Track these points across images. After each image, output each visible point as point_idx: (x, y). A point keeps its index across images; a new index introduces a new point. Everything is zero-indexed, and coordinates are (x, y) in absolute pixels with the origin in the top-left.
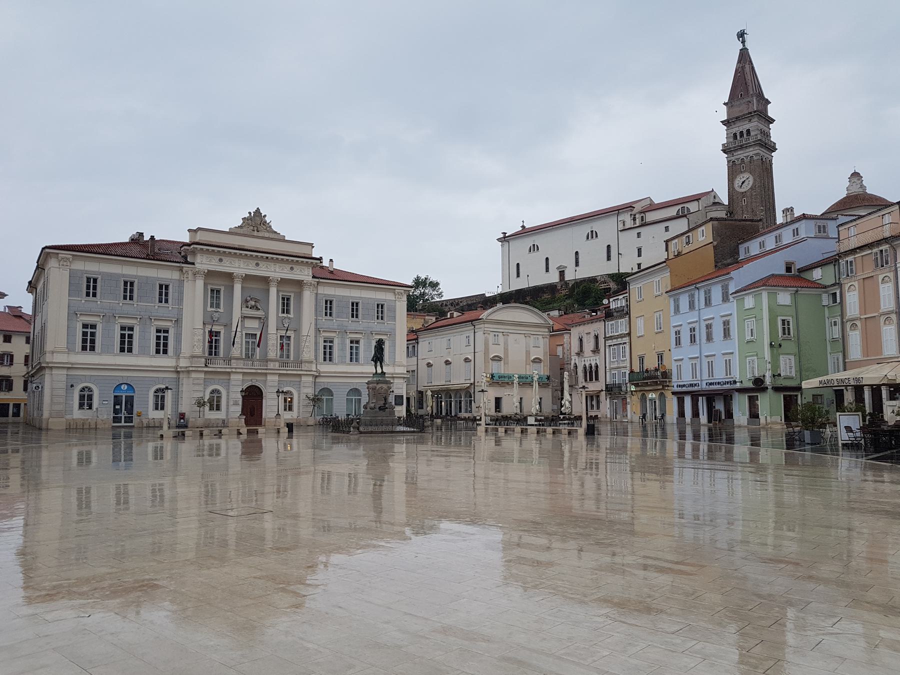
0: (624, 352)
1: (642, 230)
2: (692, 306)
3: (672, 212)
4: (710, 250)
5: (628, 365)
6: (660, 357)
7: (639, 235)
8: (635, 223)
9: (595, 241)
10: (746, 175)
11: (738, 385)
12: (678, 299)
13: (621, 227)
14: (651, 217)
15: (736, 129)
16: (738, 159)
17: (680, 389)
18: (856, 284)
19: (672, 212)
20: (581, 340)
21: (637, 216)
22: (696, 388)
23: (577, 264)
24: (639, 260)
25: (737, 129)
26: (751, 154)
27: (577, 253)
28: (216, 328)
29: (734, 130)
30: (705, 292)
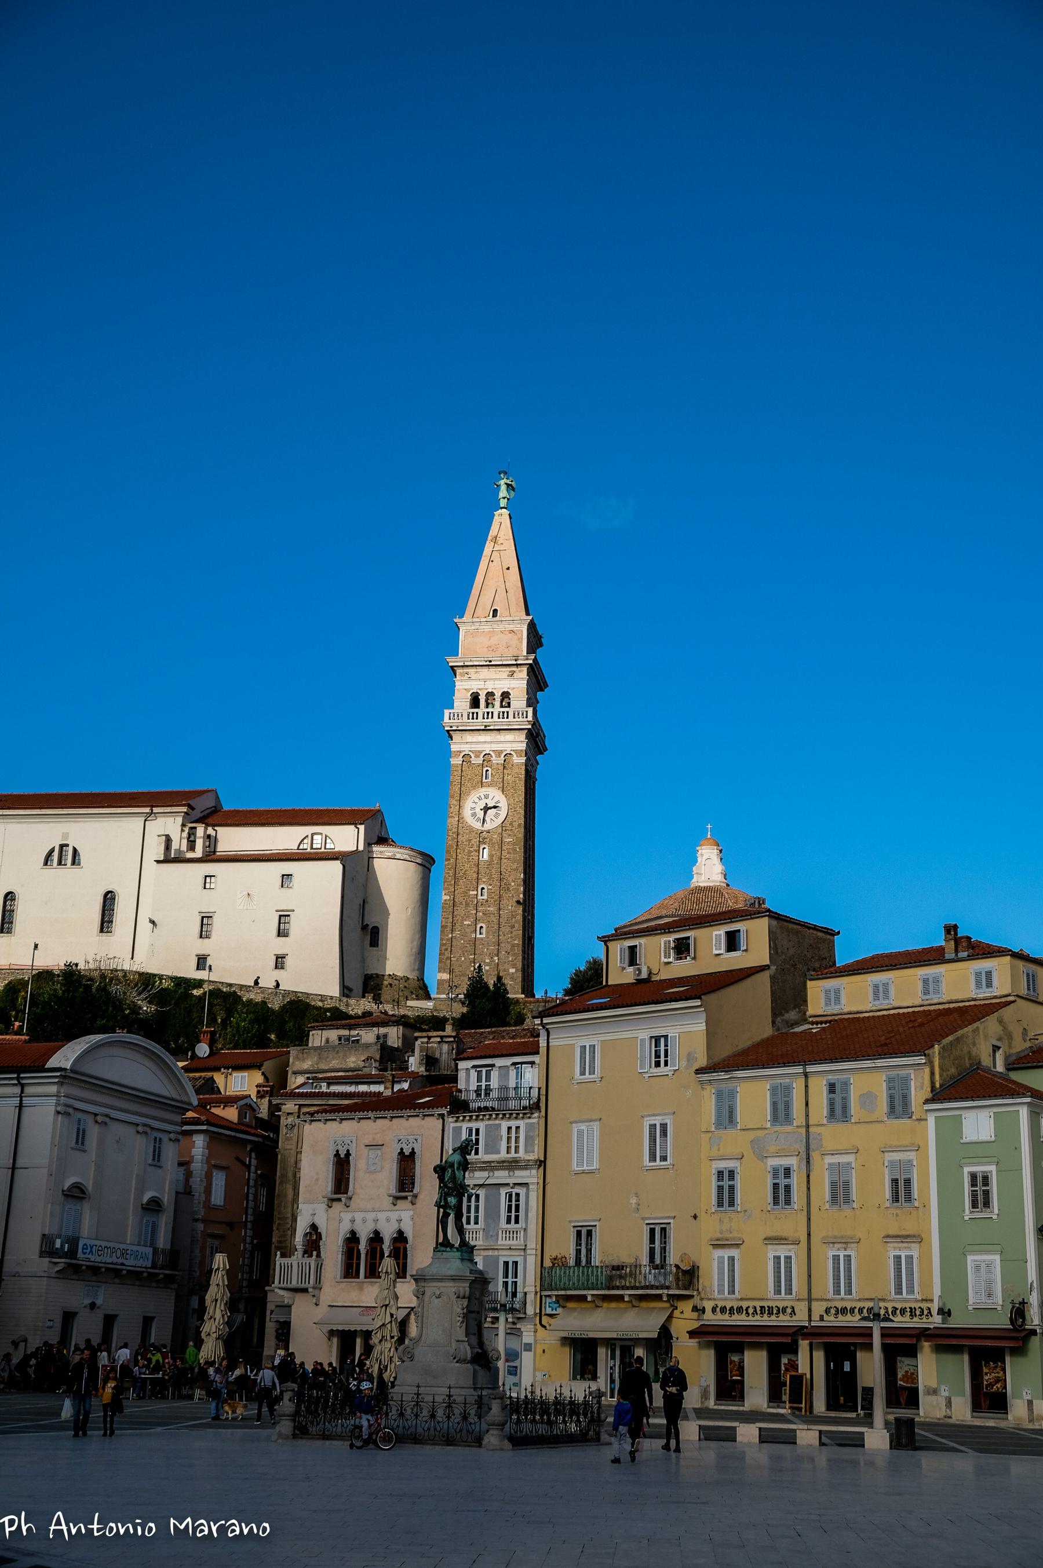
0: (514, 1213)
2: (781, 1112)
4: (763, 983)
5: (533, 1244)
6: (658, 1234)
8: (192, 847)
9: (68, 872)
10: (495, 796)
11: (937, 1320)
12: (732, 1094)
13: (155, 850)
16: (477, 754)
17: (725, 1319)
20: (342, 1164)
21: (200, 831)
22: (784, 1320)
26: (508, 748)
29: (475, 686)
30: (832, 1088)
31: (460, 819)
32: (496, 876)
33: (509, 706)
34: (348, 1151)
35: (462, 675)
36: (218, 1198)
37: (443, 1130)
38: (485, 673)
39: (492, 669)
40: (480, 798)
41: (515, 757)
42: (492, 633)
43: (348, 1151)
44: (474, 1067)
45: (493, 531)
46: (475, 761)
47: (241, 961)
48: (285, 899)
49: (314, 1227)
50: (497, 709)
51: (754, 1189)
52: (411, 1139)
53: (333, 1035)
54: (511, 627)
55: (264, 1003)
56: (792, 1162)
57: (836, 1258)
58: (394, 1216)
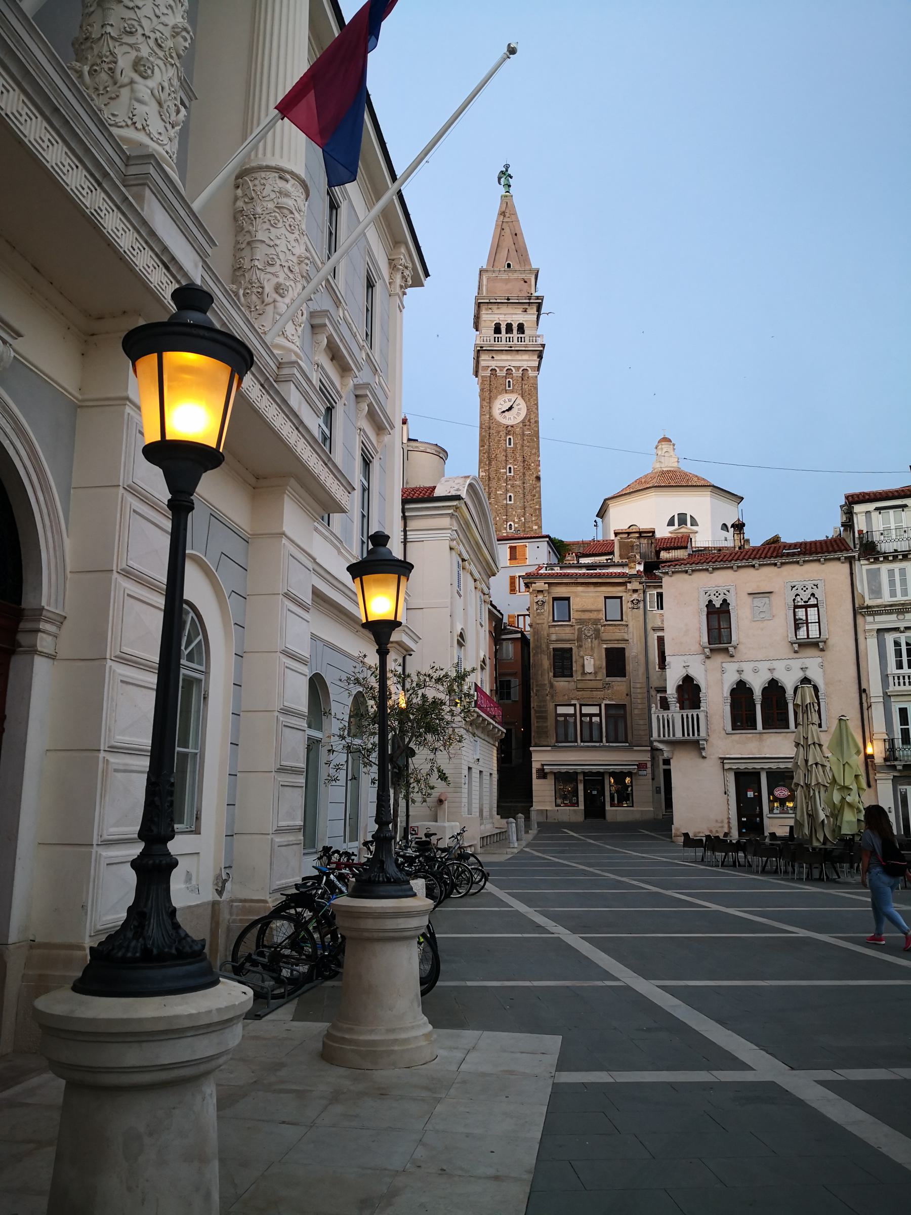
16: (501, 368)
25: (502, 317)
26: (525, 365)
31: (491, 416)
32: (520, 459)
33: (523, 333)
34: (725, 600)
35: (486, 309)
37: (852, 574)
38: (504, 309)
39: (510, 306)
40: (505, 401)
41: (530, 371)
42: (507, 281)
43: (725, 600)
44: (877, 509)
46: (498, 373)
49: (688, 679)
50: (515, 334)
52: (809, 585)
54: (523, 276)
58: (796, 664)
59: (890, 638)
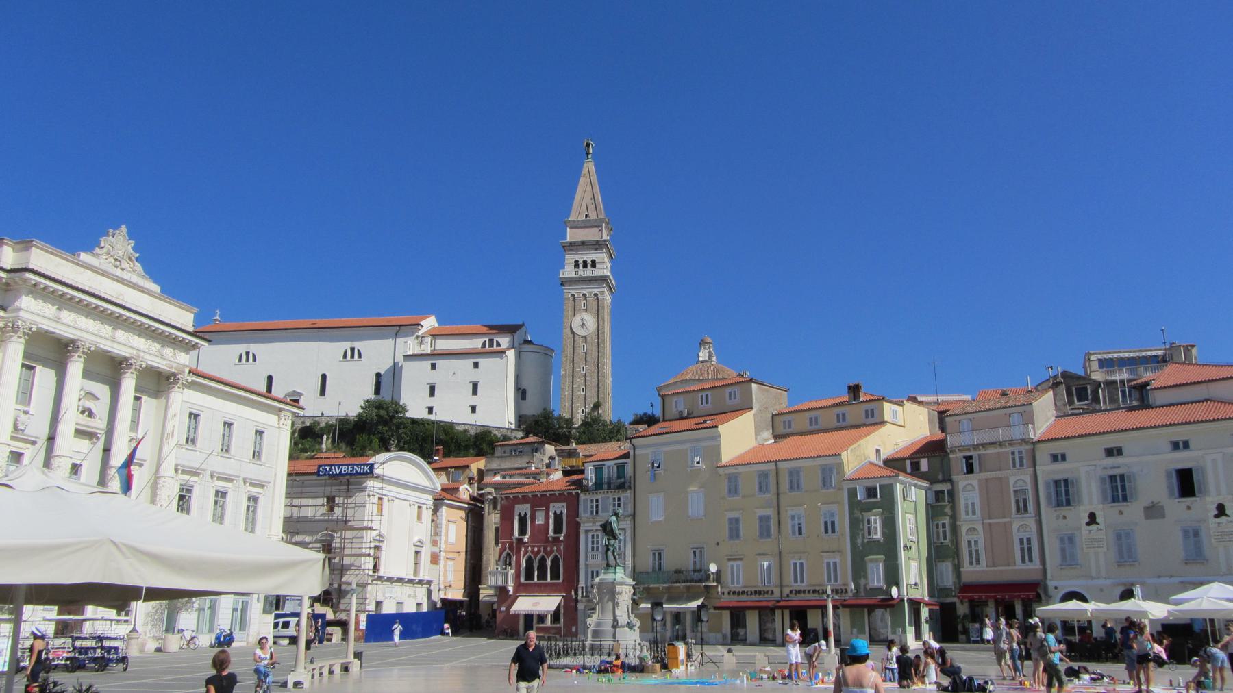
1: (440, 363)
2: (762, 488)
3: (476, 344)
7: (434, 366)
14: (443, 345)
15: (580, 258)
18: (975, 483)
19: (476, 344)
22: (767, 597)
23: (323, 393)
24: (431, 402)
26: (596, 291)
27: (324, 377)
28: (18, 446)
29: (577, 257)
30: (791, 473)
36: (452, 538)
45: (585, 171)
47: (452, 409)
48: (475, 375)
51: (749, 528)
53: (508, 449)
55: (466, 431)
56: (770, 512)
57: (795, 564)
59: (590, 535)
